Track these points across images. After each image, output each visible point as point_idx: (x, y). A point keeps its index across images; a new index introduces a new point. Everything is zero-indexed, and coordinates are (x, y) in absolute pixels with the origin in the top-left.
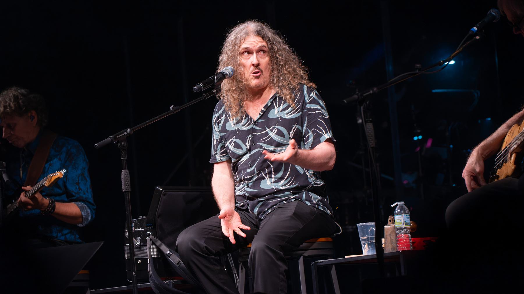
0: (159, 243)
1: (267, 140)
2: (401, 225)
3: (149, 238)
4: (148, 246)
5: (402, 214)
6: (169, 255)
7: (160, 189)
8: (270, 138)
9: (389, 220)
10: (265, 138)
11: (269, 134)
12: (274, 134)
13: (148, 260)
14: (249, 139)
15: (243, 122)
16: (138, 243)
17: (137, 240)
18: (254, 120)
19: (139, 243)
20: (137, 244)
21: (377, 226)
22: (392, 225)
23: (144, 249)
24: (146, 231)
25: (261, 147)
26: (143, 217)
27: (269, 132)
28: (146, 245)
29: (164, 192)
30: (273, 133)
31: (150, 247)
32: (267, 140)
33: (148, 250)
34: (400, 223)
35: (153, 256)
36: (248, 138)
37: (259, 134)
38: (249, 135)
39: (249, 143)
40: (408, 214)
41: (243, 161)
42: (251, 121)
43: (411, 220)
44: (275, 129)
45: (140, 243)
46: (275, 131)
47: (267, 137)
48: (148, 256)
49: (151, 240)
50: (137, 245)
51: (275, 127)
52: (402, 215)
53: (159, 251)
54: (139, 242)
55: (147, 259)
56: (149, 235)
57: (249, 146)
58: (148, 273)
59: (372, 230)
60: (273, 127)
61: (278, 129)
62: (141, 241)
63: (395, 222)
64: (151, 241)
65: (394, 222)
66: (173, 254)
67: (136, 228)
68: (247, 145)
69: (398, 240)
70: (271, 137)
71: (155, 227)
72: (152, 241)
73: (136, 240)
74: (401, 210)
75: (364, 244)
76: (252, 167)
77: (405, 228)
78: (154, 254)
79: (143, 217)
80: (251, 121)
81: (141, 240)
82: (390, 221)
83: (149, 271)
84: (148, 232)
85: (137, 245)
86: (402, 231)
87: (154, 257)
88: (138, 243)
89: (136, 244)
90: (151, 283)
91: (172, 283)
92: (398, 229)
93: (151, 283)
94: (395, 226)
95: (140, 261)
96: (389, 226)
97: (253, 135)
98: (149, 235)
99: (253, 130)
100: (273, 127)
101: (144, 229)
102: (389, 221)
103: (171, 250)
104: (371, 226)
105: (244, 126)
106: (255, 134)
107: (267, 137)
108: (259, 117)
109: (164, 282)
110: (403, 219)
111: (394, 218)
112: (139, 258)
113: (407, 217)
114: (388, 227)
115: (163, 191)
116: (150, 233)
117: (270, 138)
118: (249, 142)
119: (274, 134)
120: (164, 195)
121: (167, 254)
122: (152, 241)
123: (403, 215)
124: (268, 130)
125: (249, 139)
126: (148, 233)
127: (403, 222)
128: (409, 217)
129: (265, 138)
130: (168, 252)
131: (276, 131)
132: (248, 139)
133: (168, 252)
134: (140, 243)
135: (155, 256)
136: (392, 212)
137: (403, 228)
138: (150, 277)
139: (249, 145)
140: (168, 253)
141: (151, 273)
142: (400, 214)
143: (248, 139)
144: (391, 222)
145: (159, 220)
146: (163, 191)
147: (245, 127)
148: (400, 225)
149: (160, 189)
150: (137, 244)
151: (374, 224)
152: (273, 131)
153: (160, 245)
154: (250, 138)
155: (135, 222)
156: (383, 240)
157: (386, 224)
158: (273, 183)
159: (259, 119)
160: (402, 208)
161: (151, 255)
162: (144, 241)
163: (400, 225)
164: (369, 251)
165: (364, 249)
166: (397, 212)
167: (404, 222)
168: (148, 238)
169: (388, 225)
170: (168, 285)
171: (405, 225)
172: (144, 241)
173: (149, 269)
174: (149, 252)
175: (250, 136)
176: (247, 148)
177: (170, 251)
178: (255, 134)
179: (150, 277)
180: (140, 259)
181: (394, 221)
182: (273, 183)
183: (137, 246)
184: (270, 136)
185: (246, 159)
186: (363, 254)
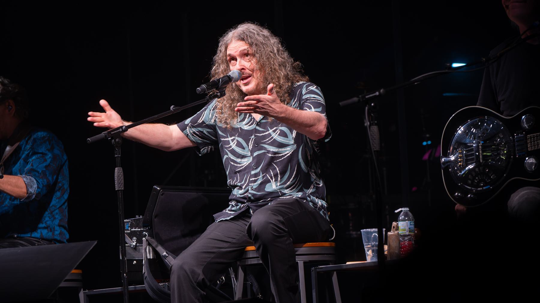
0: (154, 243)
2: (405, 232)
3: (145, 238)
4: (144, 247)
5: (406, 220)
6: (165, 257)
7: (158, 188)
8: (273, 139)
9: (393, 226)
10: (268, 139)
12: (277, 135)
13: (144, 261)
14: (252, 140)
15: (246, 120)
16: (133, 244)
17: (133, 241)
18: (256, 121)
19: (134, 244)
21: (380, 233)
22: (396, 232)
23: (140, 249)
24: (142, 231)
26: (139, 217)
27: (272, 133)
28: (142, 246)
29: (162, 191)
30: (276, 134)
31: (146, 248)
32: (270, 141)
33: (143, 251)
34: (404, 230)
35: (148, 257)
36: (251, 138)
37: (261, 135)
38: (252, 136)
39: (252, 144)
40: (413, 220)
42: (254, 121)
43: (415, 227)
44: (278, 130)
45: (136, 244)
46: (278, 132)
47: (270, 138)
48: (144, 258)
49: (147, 240)
50: (132, 246)
51: (278, 128)
52: (406, 221)
53: (156, 252)
54: (135, 243)
55: (143, 260)
56: (145, 236)
57: (251, 147)
58: (143, 275)
59: (375, 235)
60: (276, 128)
61: (281, 130)
62: (137, 241)
63: (399, 228)
64: (148, 242)
65: (397, 228)
66: (170, 256)
67: (132, 228)
68: (250, 146)
69: (401, 248)
70: (274, 138)
71: (151, 228)
72: (149, 242)
73: (132, 240)
74: (405, 217)
75: (368, 251)
77: (409, 235)
78: (150, 256)
79: (139, 217)
80: (254, 121)
81: (136, 240)
82: (394, 227)
83: (145, 273)
84: (144, 233)
85: (132, 246)
86: (406, 238)
87: (150, 259)
88: (133, 244)
89: (132, 245)
90: (145, 286)
91: (168, 286)
92: (402, 236)
93: (145, 286)
94: (398, 233)
95: (135, 262)
96: (393, 233)
97: (255, 136)
98: (145, 236)
99: (255, 131)
100: (276, 128)
101: (140, 229)
102: (392, 227)
103: (167, 252)
104: (374, 232)
105: (247, 126)
106: (258, 135)
107: (270, 138)
108: (262, 118)
109: (160, 284)
110: (407, 226)
111: (398, 224)
112: (134, 259)
113: (411, 223)
114: (391, 233)
115: (161, 191)
116: (146, 233)
117: (273, 139)
118: (252, 142)
119: (277, 135)
120: (162, 195)
121: (163, 256)
122: (149, 242)
123: (408, 221)
124: (271, 131)
125: (252, 140)
126: (144, 234)
127: (407, 228)
128: (412, 223)
129: (268, 139)
130: (165, 253)
131: (279, 132)
132: (251, 140)
133: (165, 253)
134: (136, 243)
135: (151, 258)
136: (396, 218)
137: (407, 235)
138: (146, 278)
139: (252, 146)
140: (165, 255)
141: (146, 275)
142: (404, 220)
143: (251, 140)
144: (395, 229)
145: (156, 220)
146: (161, 191)
147: (247, 127)
148: (404, 232)
149: (158, 188)
150: (132, 244)
151: (376, 230)
152: (276, 132)
153: (157, 246)
154: (253, 138)
155: (131, 221)
156: (386, 247)
157: (390, 231)
159: (262, 119)
160: (406, 215)
162: (139, 241)
163: (404, 232)
164: (371, 259)
165: (368, 256)
166: (401, 218)
167: (408, 229)
168: (144, 238)
169: (392, 231)
170: (164, 287)
171: (409, 232)
172: (139, 241)
173: (145, 270)
174: (145, 253)
175: (253, 137)
176: (249, 148)
177: (166, 253)
178: (258, 135)
179: (146, 278)
180: (135, 260)
181: (398, 227)
184: (272, 138)
186: (366, 261)
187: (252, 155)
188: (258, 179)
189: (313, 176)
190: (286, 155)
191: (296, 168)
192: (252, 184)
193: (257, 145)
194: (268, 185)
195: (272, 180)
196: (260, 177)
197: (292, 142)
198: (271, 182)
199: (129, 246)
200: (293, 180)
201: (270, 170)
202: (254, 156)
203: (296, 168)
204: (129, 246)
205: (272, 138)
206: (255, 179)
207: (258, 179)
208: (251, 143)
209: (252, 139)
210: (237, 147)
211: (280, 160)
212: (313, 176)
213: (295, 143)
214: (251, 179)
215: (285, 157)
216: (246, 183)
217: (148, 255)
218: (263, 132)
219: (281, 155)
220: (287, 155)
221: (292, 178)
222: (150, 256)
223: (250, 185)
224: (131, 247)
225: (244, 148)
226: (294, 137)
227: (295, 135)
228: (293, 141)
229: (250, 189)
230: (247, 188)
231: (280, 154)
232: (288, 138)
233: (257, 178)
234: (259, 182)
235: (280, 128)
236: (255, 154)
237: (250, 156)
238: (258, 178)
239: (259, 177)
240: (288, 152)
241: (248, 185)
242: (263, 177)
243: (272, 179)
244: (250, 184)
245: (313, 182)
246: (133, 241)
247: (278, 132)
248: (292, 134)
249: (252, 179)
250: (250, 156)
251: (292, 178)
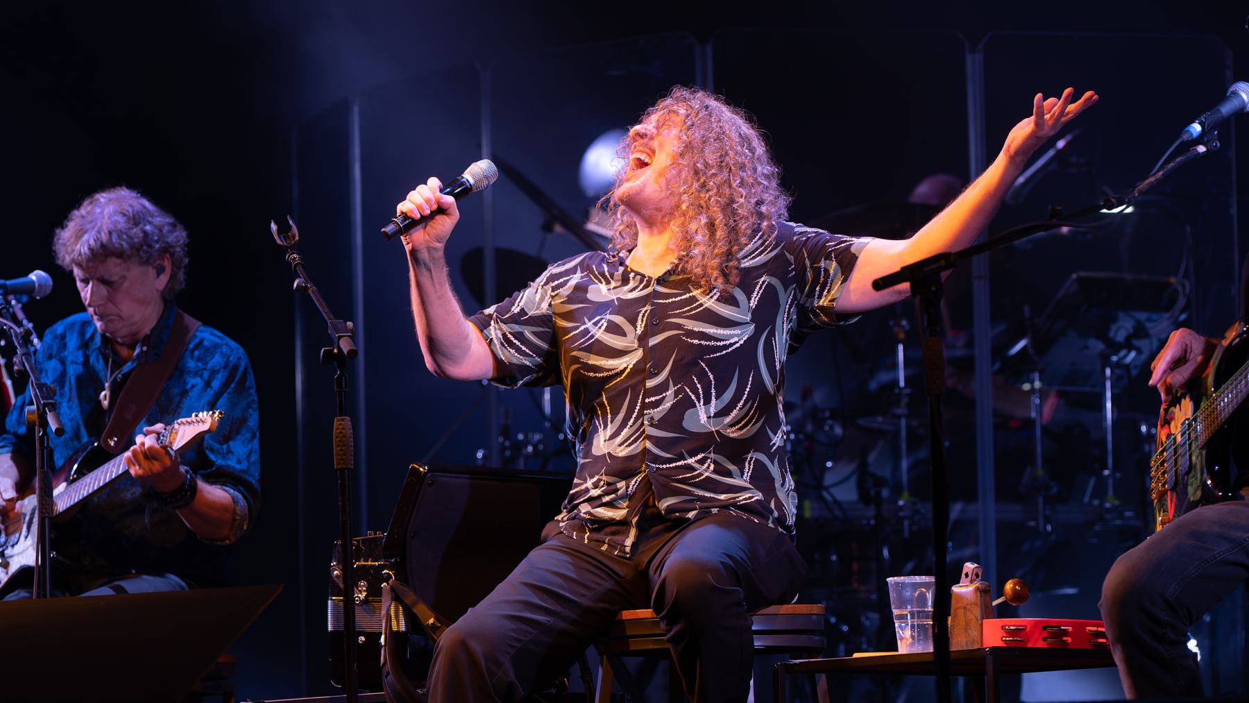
27: (591, 329)
35: (395, 628)
60: (599, 317)
61: (609, 322)
78: (400, 625)
87: (398, 632)
100: (599, 317)
124: (589, 325)
135: (403, 628)
161: (391, 625)
188: (664, 397)
191: (750, 379)
192: (651, 411)
195: (699, 403)
196: (670, 392)
200: (744, 406)
201: (694, 377)
203: (750, 379)
206: (657, 398)
207: (664, 397)
211: (718, 354)
214: (647, 401)
215: (730, 350)
216: (636, 411)
217: (394, 623)
218: (577, 328)
220: (734, 347)
221: (742, 402)
222: (400, 625)
223: (646, 414)
229: (646, 422)
230: (640, 421)
231: (720, 340)
233: (661, 396)
234: (668, 405)
235: (608, 317)
237: (636, 349)
238: (664, 394)
239: (667, 393)
240: (736, 339)
241: (641, 414)
242: (676, 393)
244: (645, 412)
247: (602, 325)
249: (650, 400)
250: (636, 349)
251: (742, 402)
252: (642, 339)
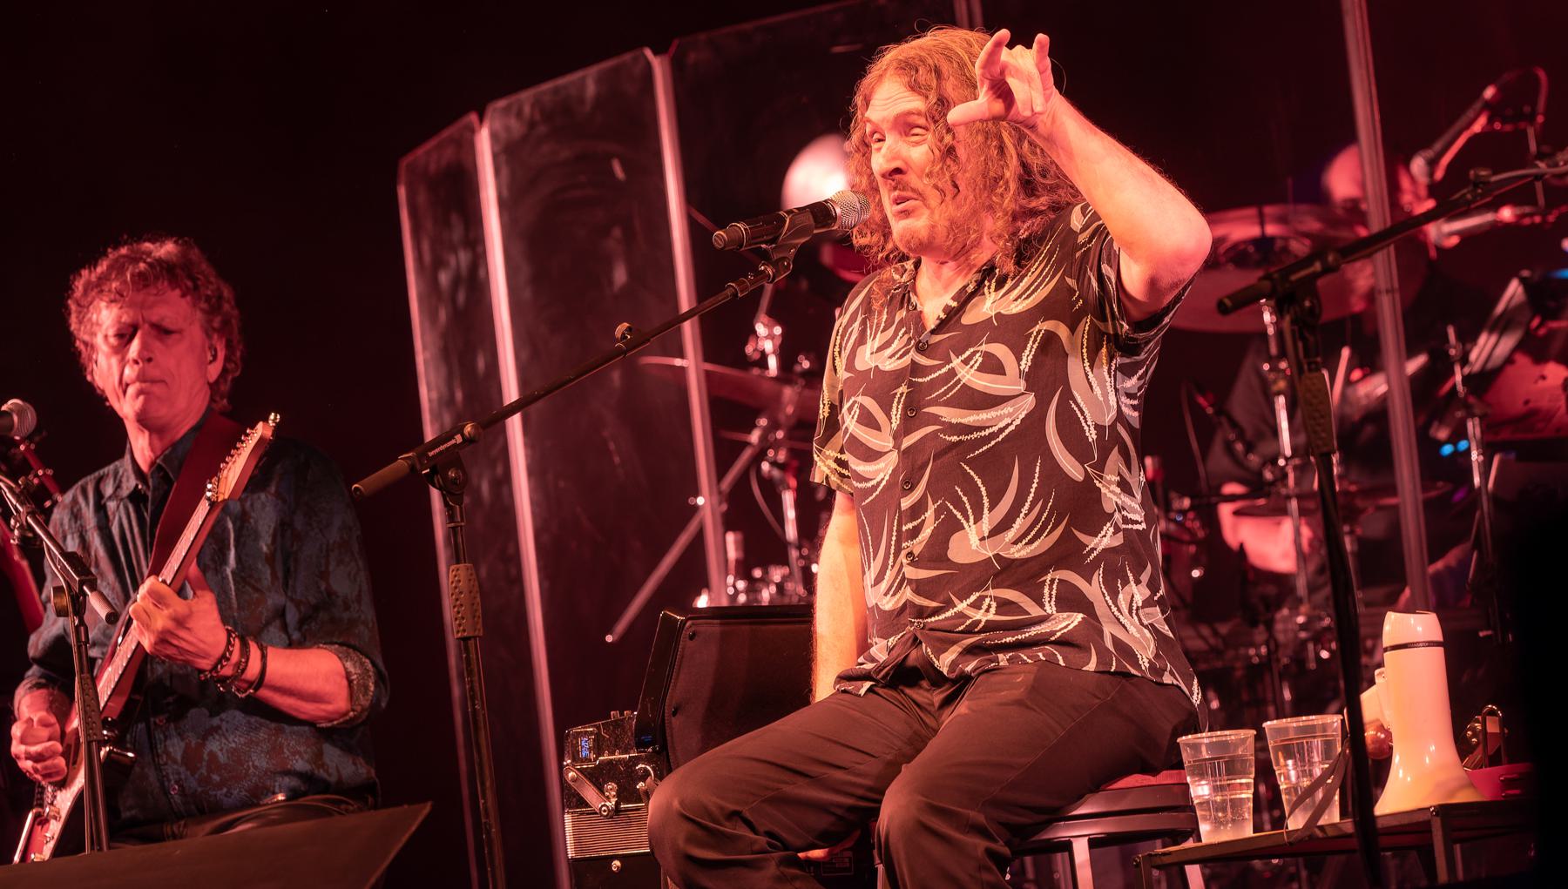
1: (950, 394)
8: (959, 386)
10: (945, 388)
11: (957, 375)
12: (972, 371)
16: (608, 804)
19: (611, 804)
20: (608, 807)
25: (935, 419)
32: (950, 394)
41: (883, 479)
50: (605, 811)
73: (604, 794)
76: (912, 489)
85: (605, 811)
88: (608, 804)
89: (603, 808)
117: (959, 386)
118: (900, 407)
119: (972, 371)
129: (945, 388)
134: (616, 802)
143: (896, 400)
158: (988, 537)
182: (988, 537)
183: (605, 814)
185: (890, 472)
187: (897, 446)
189: (1110, 495)
190: (1001, 430)
193: (913, 416)
194: (955, 539)
197: (1022, 386)
198: (964, 528)
199: (596, 813)
202: (904, 446)
204: (596, 813)
205: (959, 380)
208: (897, 408)
209: (898, 395)
210: (863, 427)
212: (1110, 495)
213: (1029, 389)
219: (987, 432)
224: (602, 815)
225: (878, 428)
226: (1027, 370)
227: (1029, 364)
228: (1023, 382)
232: (1005, 374)
236: (908, 442)
243: (967, 520)
245: (1112, 515)
246: (607, 794)
248: (1019, 359)
252: (898, 436)
